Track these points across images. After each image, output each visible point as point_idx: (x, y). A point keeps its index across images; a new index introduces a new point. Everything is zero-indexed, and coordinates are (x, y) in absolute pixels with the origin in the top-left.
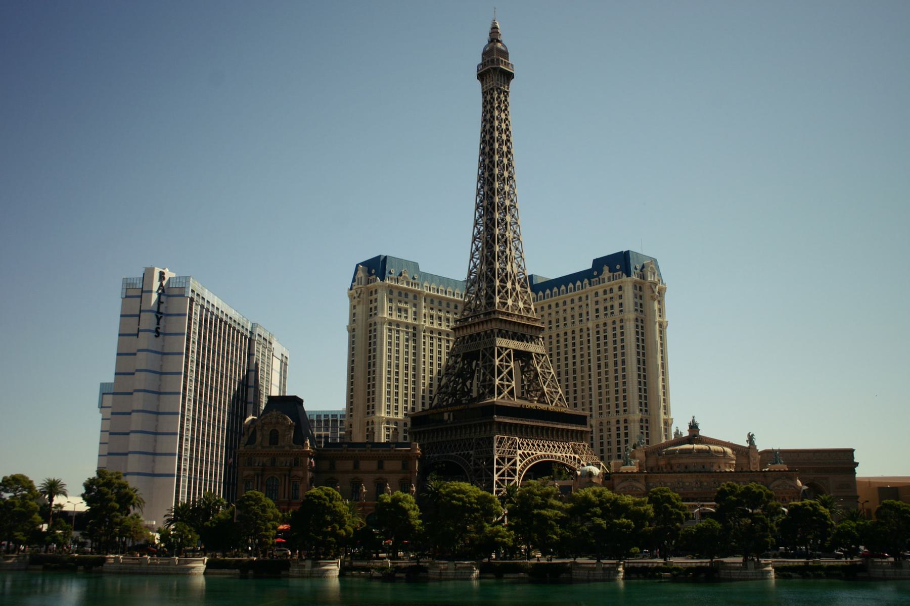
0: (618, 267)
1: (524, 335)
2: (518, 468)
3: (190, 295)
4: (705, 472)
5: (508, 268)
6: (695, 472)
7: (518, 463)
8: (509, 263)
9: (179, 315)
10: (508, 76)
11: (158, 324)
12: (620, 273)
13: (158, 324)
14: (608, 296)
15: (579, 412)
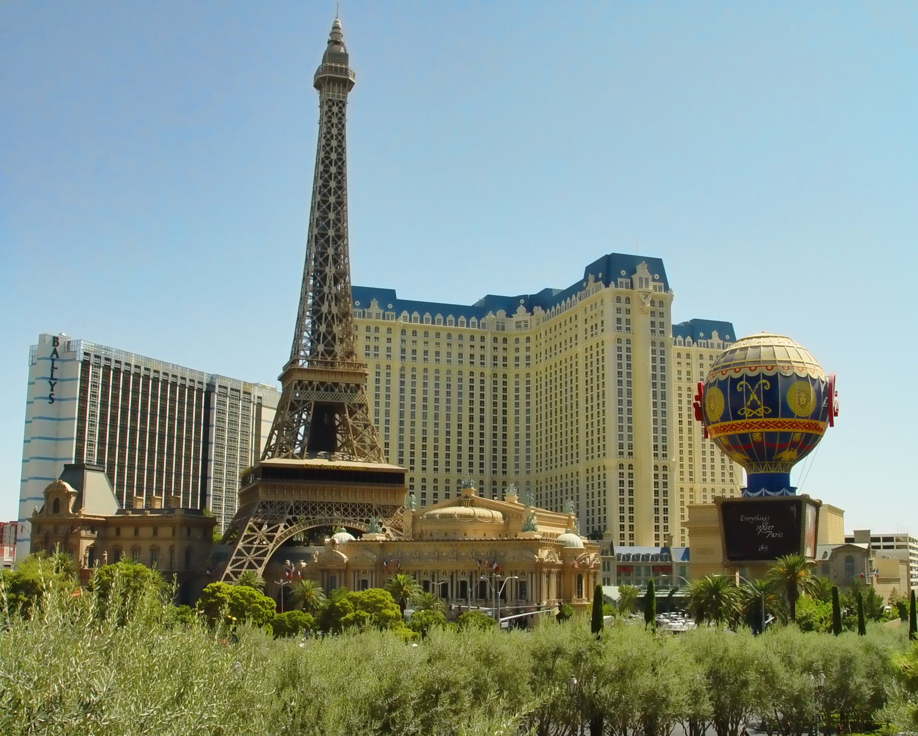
0: (600, 275)
1: (336, 385)
2: (278, 535)
3: (82, 357)
4: (449, 540)
5: (324, 309)
6: (438, 540)
7: (281, 528)
8: (326, 303)
9: (72, 379)
10: (347, 85)
11: (52, 390)
12: (601, 282)
13: (52, 390)
14: (594, 311)
15: (393, 466)
